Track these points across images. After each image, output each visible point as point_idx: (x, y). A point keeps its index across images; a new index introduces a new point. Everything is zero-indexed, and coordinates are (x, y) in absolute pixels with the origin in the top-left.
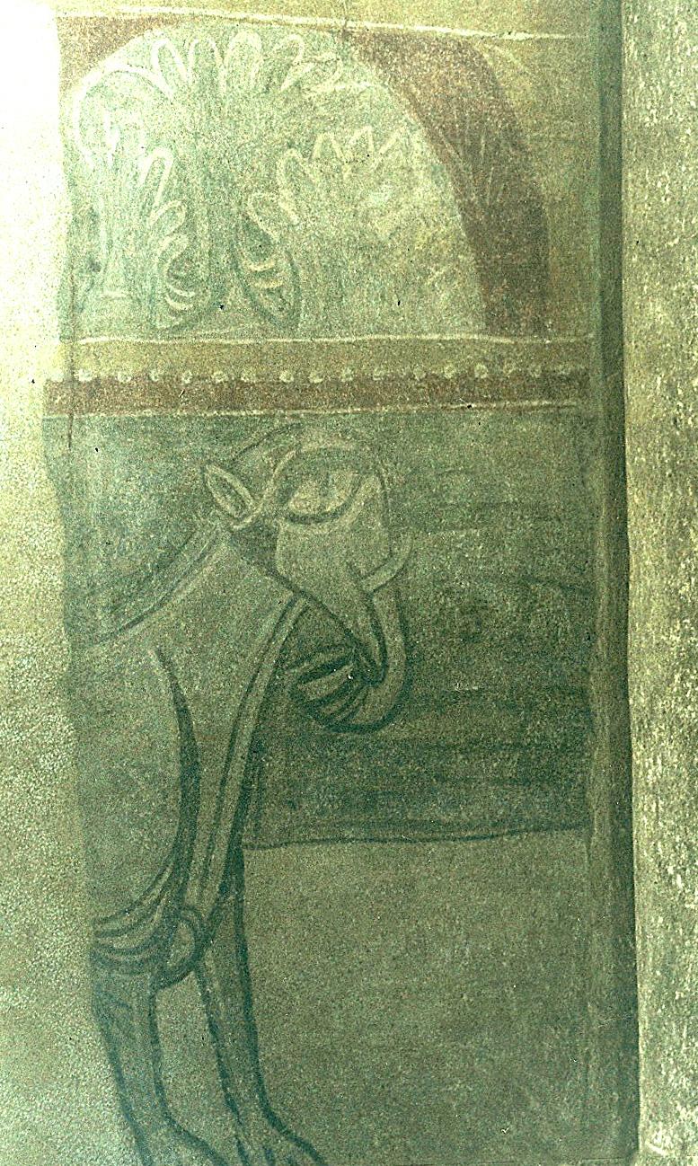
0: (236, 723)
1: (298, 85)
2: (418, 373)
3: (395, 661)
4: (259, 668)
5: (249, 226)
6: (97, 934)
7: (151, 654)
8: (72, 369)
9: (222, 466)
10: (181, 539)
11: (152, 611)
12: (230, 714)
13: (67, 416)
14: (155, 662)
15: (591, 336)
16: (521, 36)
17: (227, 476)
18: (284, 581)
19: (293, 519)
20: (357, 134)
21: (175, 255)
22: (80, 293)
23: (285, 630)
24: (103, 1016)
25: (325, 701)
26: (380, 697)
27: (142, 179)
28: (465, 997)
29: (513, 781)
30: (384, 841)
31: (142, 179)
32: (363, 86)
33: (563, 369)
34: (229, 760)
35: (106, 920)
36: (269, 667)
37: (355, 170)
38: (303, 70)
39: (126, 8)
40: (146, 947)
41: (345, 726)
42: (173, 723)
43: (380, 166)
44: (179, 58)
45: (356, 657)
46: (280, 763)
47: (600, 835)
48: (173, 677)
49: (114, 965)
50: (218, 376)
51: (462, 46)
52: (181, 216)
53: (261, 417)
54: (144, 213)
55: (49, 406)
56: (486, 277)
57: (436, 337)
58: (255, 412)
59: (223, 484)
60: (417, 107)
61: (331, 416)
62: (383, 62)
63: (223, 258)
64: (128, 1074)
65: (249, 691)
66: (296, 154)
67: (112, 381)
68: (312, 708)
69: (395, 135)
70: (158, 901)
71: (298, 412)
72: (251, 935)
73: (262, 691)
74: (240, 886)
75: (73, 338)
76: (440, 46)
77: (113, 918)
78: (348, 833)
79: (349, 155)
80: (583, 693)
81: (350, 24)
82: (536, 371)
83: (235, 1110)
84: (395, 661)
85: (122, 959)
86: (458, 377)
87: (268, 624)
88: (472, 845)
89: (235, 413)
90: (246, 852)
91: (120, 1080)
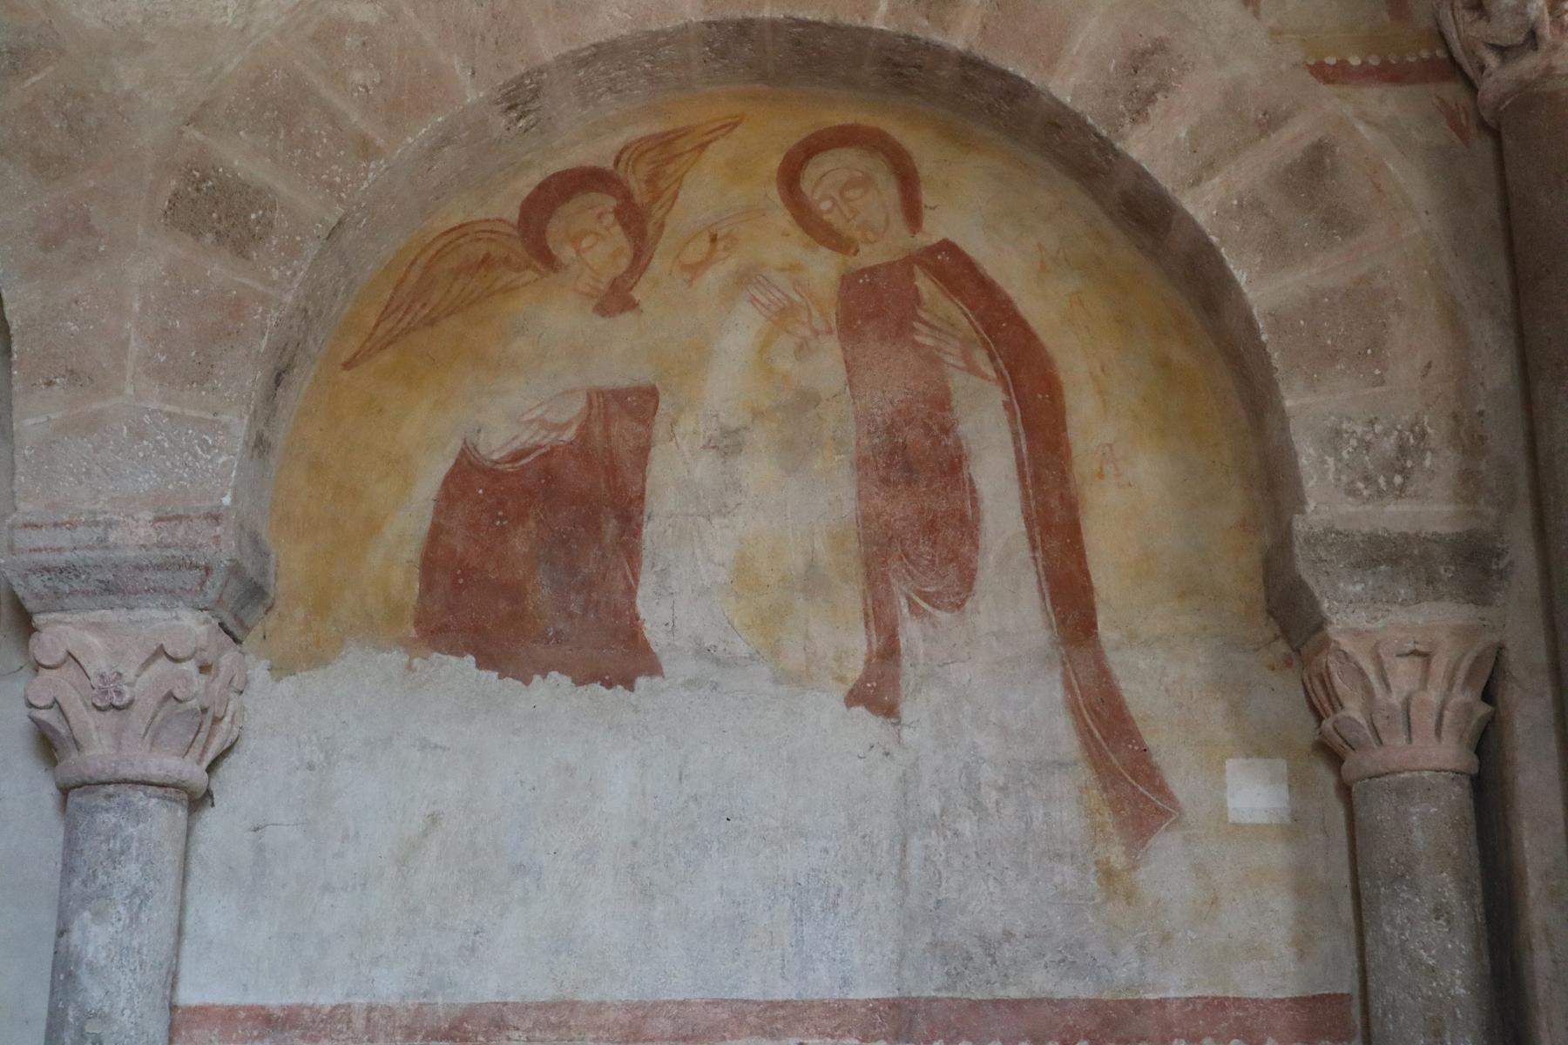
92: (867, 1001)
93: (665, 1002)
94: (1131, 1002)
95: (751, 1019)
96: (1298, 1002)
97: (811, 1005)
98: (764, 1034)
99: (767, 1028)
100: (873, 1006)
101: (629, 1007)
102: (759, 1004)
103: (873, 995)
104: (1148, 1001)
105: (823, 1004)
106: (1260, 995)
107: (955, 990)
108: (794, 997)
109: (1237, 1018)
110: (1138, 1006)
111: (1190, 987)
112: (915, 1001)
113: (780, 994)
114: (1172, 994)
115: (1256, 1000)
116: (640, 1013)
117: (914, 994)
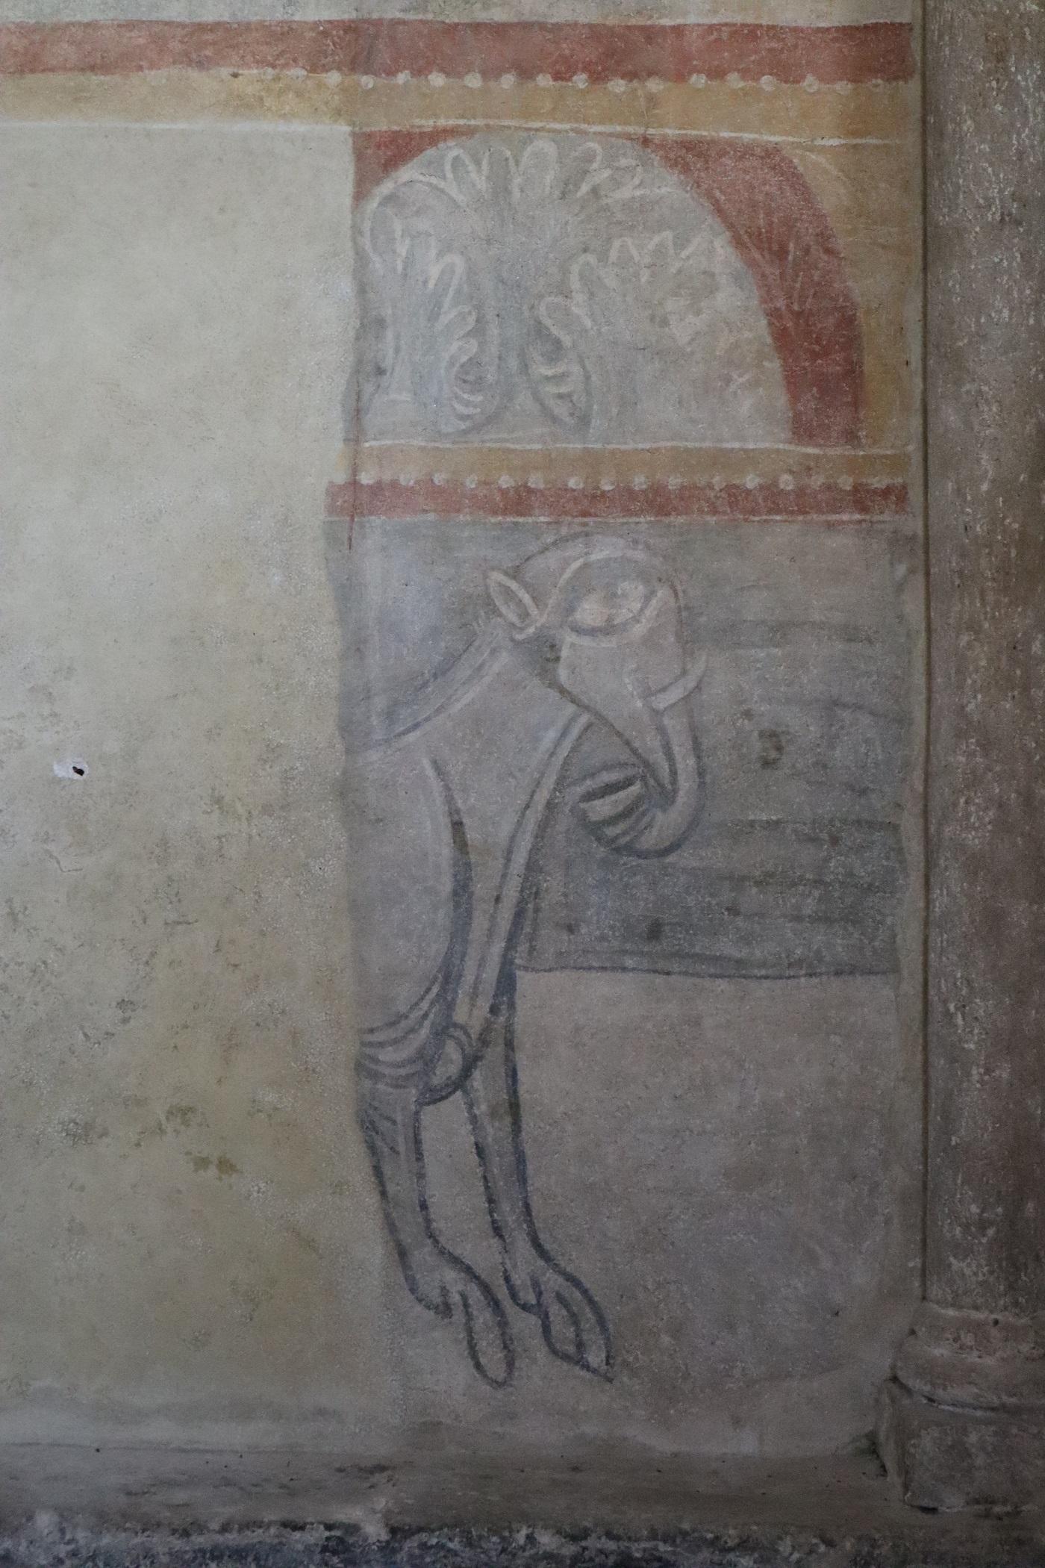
0: (513, 838)
1: (595, 191)
2: (718, 481)
3: (686, 784)
4: (538, 784)
5: (540, 331)
6: (363, 1044)
7: (426, 763)
8: (355, 470)
9: (506, 574)
10: (461, 647)
11: (427, 719)
13: (348, 519)
14: (430, 772)
15: (911, 448)
16: (835, 142)
17: (514, 585)
18: (563, 691)
19: (578, 630)
20: (657, 239)
21: (464, 359)
22: (365, 398)
24: (367, 1127)
26: (665, 823)
27: (431, 285)
28: (753, 1145)
29: (815, 919)
30: (668, 973)
31: (431, 285)
32: (664, 190)
33: (878, 482)
34: (504, 876)
35: (372, 1031)
36: (550, 782)
37: (653, 275)
38: (601, 176)
39: (418, 122)
40: (411, 1061)
41: (629, 849)
42: (447, 836)
43: (679, 272)
44: (471, 167)
45: (643, 778)
46: (558, 885)
47: (911, 987)
48: (447, 788)
49: (375, 1076)
50: (505, 481)
51: (770, 153)
52: (471, 320)
53: (549, 523)
54: (433, 317)
55: (332, 509)
56: (794, 383)
57: (737, 445)
58: (542, 519)
59: (508, 593)
60: (719, 211)
61: (623, 524)
62: (686, 169)
63: (513, 363)
64: (391, 1189)
65: (527, 806)
66: (591, 258)
67: (394, 484)
68: (595, 829)
69: (696, 241)
70: (425, 1016)
71: (585, 520)
72: (522, 1059)
73: (540, 808)
74: (512, 1006)
75: (357, 441)
76: (745, 152)
78: (630, 962)
79: (647, 260)
80: (895, 828)
81: (651, 131)
82: (846, 482)
83: (501, 1237)
84: (686, 784)
85: (387, 1071)
86: (761, 487)
87: (552, 735)
88: (766, 983)
89: (521, 520)
90: (518, 973)
91: (383, 1194)
92: (318, 24)
93: (68, 25)
94: (643, 29)
95: (175, 45)
96: (848, 32)
97: (248, 27)
98: (190, 63)
99: (194, 56)
100: (325, 31)
101: (24, 30)
102: (183, 26)
103: (326, 15)
104: (663, 27)
105: (262, 26)
106: (802, 23)
107: (426, 11)
108: (226, 18)
109: (770, 50)
110: (650, 34)
111: (715, 12)
112: (378, 23)
113: (209, 17)
114: (691, 19)
115: (796, 30)
116: (37, 37)
117: (375, 16)
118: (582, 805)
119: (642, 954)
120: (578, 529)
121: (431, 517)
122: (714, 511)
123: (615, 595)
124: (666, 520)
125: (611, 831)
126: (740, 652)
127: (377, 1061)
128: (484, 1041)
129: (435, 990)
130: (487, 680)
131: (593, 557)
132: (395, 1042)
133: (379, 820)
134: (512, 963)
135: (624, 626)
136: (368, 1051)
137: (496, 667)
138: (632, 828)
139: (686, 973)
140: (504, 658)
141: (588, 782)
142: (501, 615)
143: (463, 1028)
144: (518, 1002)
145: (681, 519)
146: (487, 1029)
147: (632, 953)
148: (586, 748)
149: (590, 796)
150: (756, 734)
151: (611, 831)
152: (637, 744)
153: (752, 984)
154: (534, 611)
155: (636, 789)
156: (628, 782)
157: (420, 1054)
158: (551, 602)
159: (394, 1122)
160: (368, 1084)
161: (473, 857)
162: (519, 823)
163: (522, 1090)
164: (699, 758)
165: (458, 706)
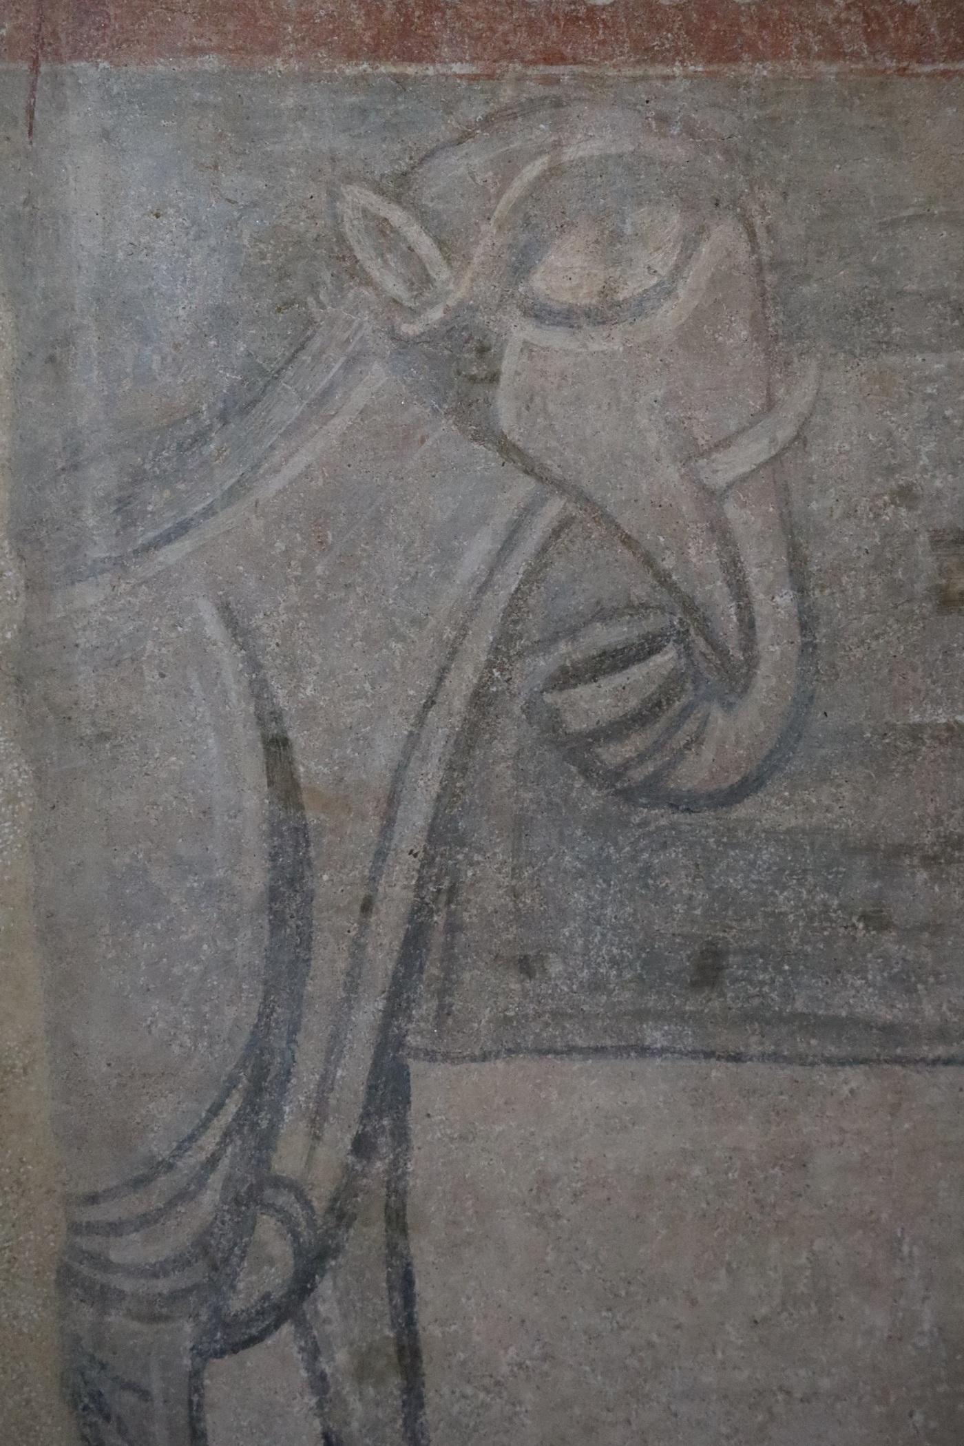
0: (399, 772)
6: (76, 1228)
7: (207, 612)
9: (380, 191)
10: (279, 350)
11: (209, 512)
12: (384, 752)
13: (25, 66)
14: (214, 629)
17: (396, 216)
18: (507, 449)
19: (538, 313)
23: (518, 565)
24: (85, 1408)
25: (618, 729)
28: (918, 1418)
30: (737, 1058)
34: (381, 855)
35: (93, 1199)
36: (478, 647)
40: (181, 1262)
42: (253, 767)
45: (682, 637)
46: (499, 871)
53: (474, 78)
58: (457, 68)
59: (382, 229)
61: (635, 80)
65: (431, 702)
70: (212, 1162)
71: (554, 70)
73: (458, 704)
74: (401, 1135)
77: (111, 1194)
78: (655, 1036)
85: (127, 1285)
89: (411, 70)
90: (415, 1067)
118: (548, 698)
119: (681, 1017)
120: (537, 90)
121: (211, 63)
122: (835, 52)
123: (617, 236)
124: (730, 71)
125: (613, 754)
126: (893, 360)
127: (107, 1266)
128: (341, 1214)
129: (232, 1107)
130: (339, 424)
131: (570, 154)
132: (145, 1221)
133: (103, 737)
134: (401, 1045)
135: (640, 306)
136: (83, 1242)
137: (360, 397)
138: (658, 746)
139: (776, 1057)
140: (377, 374)
141: (563, 647)
142: (368, 282)
143: (298, 1191)
144: (415, 1127)
145: (763, 70)
146: (348, 1187)
147: (659, 1016)
148: (558, 571)
149: (566, 678)
150: (923, 538)
151: (613, 754)
152: (668, 563)
153: (916, 1078)
154: (442, 274)
155: (666, 660)
156: (649, 647)
157: (202, 1245)
158: (478, 254)
159: (145, 1395)
160: (87, 1314)
161: (312, 817)
162: (413, 740)
163: (425, 1316)
164: (801, 590)
165: (276, 483)
